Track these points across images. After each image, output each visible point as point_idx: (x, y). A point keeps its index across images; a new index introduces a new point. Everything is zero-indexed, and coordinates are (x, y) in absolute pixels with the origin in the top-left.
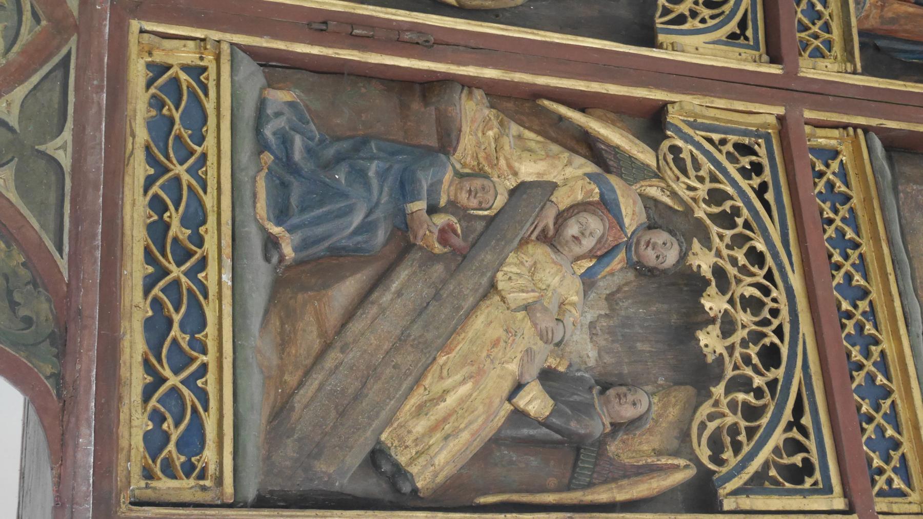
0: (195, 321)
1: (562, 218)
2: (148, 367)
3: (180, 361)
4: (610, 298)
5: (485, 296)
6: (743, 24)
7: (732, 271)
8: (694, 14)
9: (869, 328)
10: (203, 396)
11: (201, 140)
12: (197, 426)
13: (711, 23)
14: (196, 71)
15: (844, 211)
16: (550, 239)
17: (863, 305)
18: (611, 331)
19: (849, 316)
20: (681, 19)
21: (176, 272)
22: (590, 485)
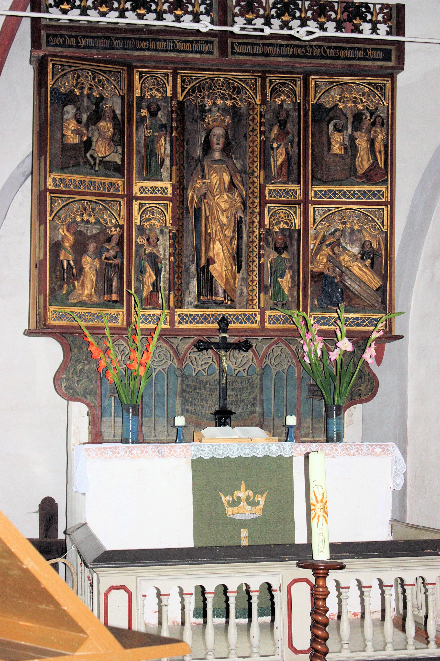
0: (357, 319)
1: (334, 253)
2: (365, 326)
3: (364, 321)
4: (346, 243)
5: (350, 270)
6: (291, 209)
7: (343, 220)
8: (290, 220)
9: (352, 192)
10: (369, 318)
11: (326, 318)
12: (374, 319)
13: (292, 217)
14: (315, 318)
15: (328, 193)
16: (337, 256)
17: (347, 193)
18: (352, 244)
19: (350, 196)
20: (292, 223)
21: (349, 322)
22: (382, 254)
